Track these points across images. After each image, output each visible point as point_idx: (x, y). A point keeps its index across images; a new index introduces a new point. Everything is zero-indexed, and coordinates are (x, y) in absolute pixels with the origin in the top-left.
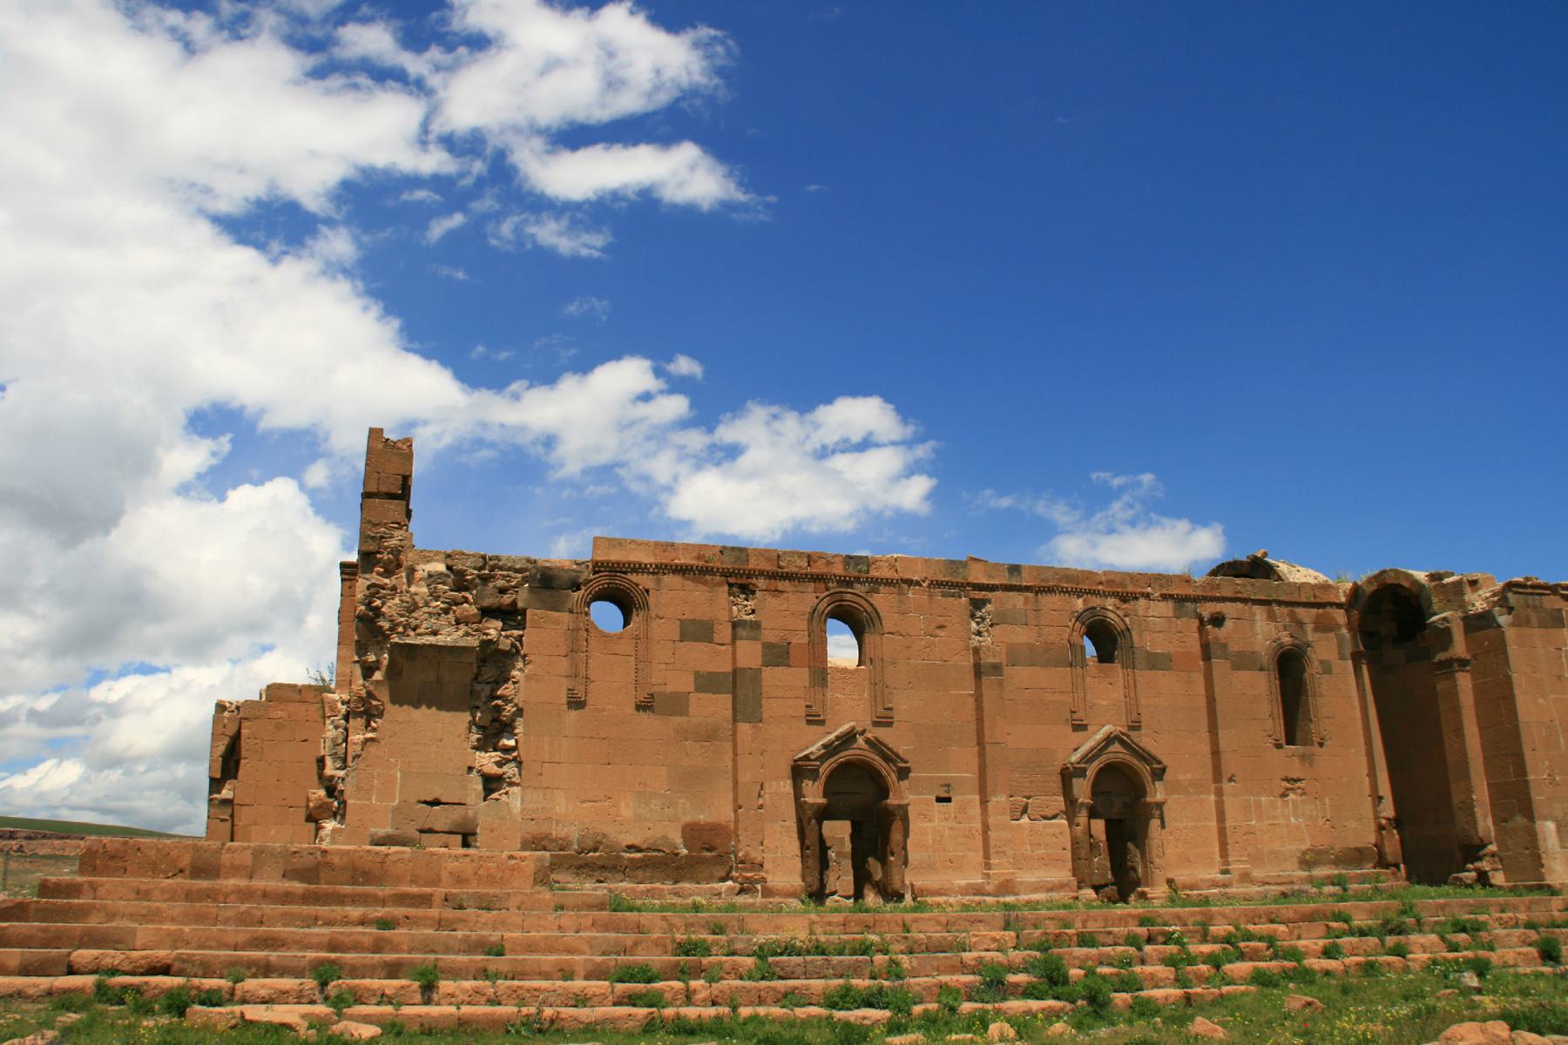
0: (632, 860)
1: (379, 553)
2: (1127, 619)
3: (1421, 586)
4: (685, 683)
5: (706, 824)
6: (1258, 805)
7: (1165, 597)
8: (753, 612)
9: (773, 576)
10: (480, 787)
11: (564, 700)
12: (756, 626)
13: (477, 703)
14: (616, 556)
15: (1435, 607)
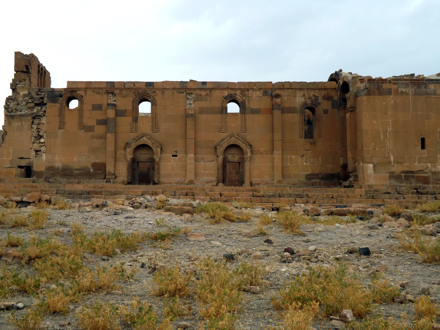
0: (77, 173)
1: (16, 89)
2: (244, 98)
3: (349, 82)
4: (92, 122)
5: (99, 163)
6: (291, 159)
7: (260, 89)
8: (115, 101)
9: (121, 90)
10: (35, 153)
11: (58, 128)
12: (115, 105)
13: (34, 130)
14: (74, 86)
15: (351, 89)
